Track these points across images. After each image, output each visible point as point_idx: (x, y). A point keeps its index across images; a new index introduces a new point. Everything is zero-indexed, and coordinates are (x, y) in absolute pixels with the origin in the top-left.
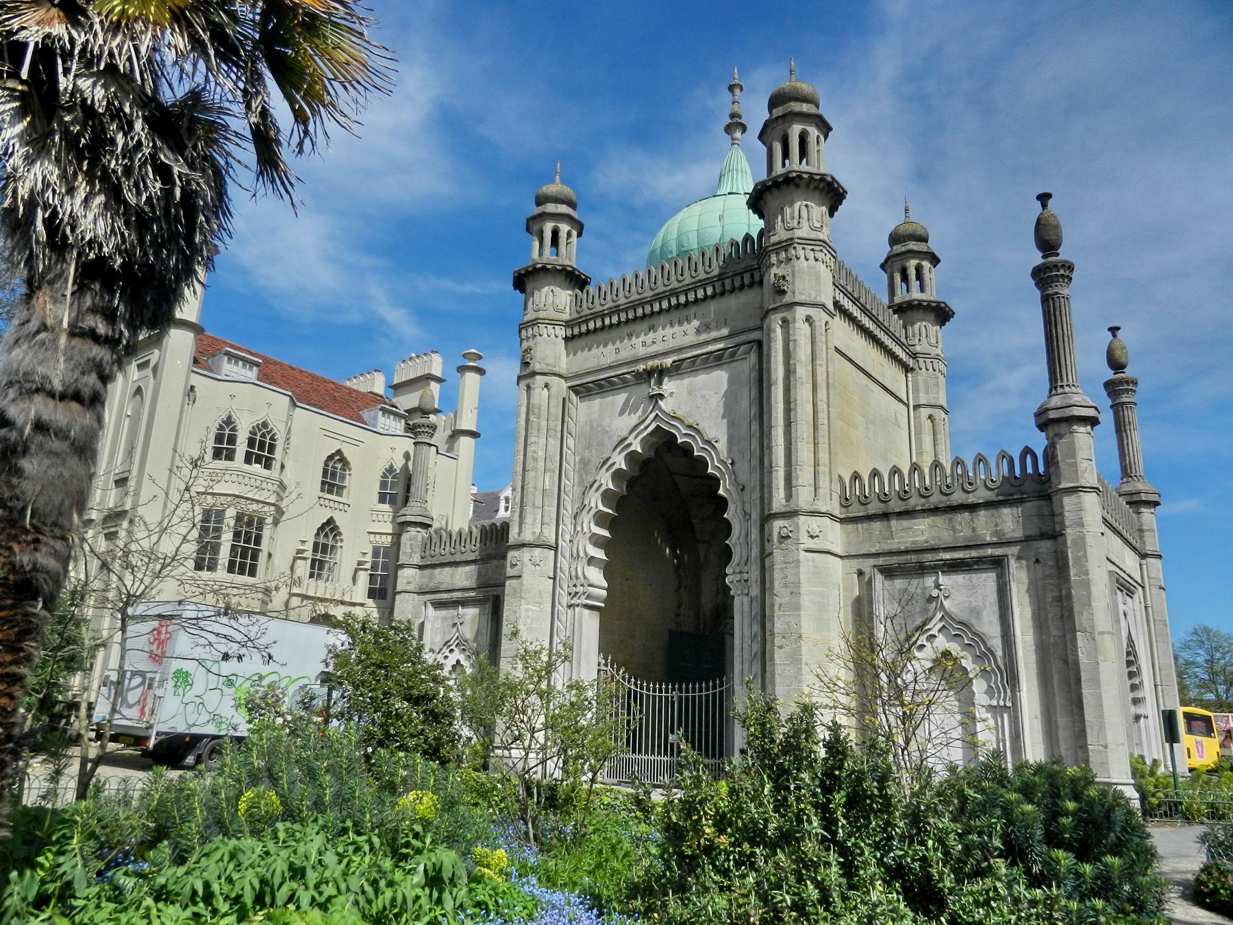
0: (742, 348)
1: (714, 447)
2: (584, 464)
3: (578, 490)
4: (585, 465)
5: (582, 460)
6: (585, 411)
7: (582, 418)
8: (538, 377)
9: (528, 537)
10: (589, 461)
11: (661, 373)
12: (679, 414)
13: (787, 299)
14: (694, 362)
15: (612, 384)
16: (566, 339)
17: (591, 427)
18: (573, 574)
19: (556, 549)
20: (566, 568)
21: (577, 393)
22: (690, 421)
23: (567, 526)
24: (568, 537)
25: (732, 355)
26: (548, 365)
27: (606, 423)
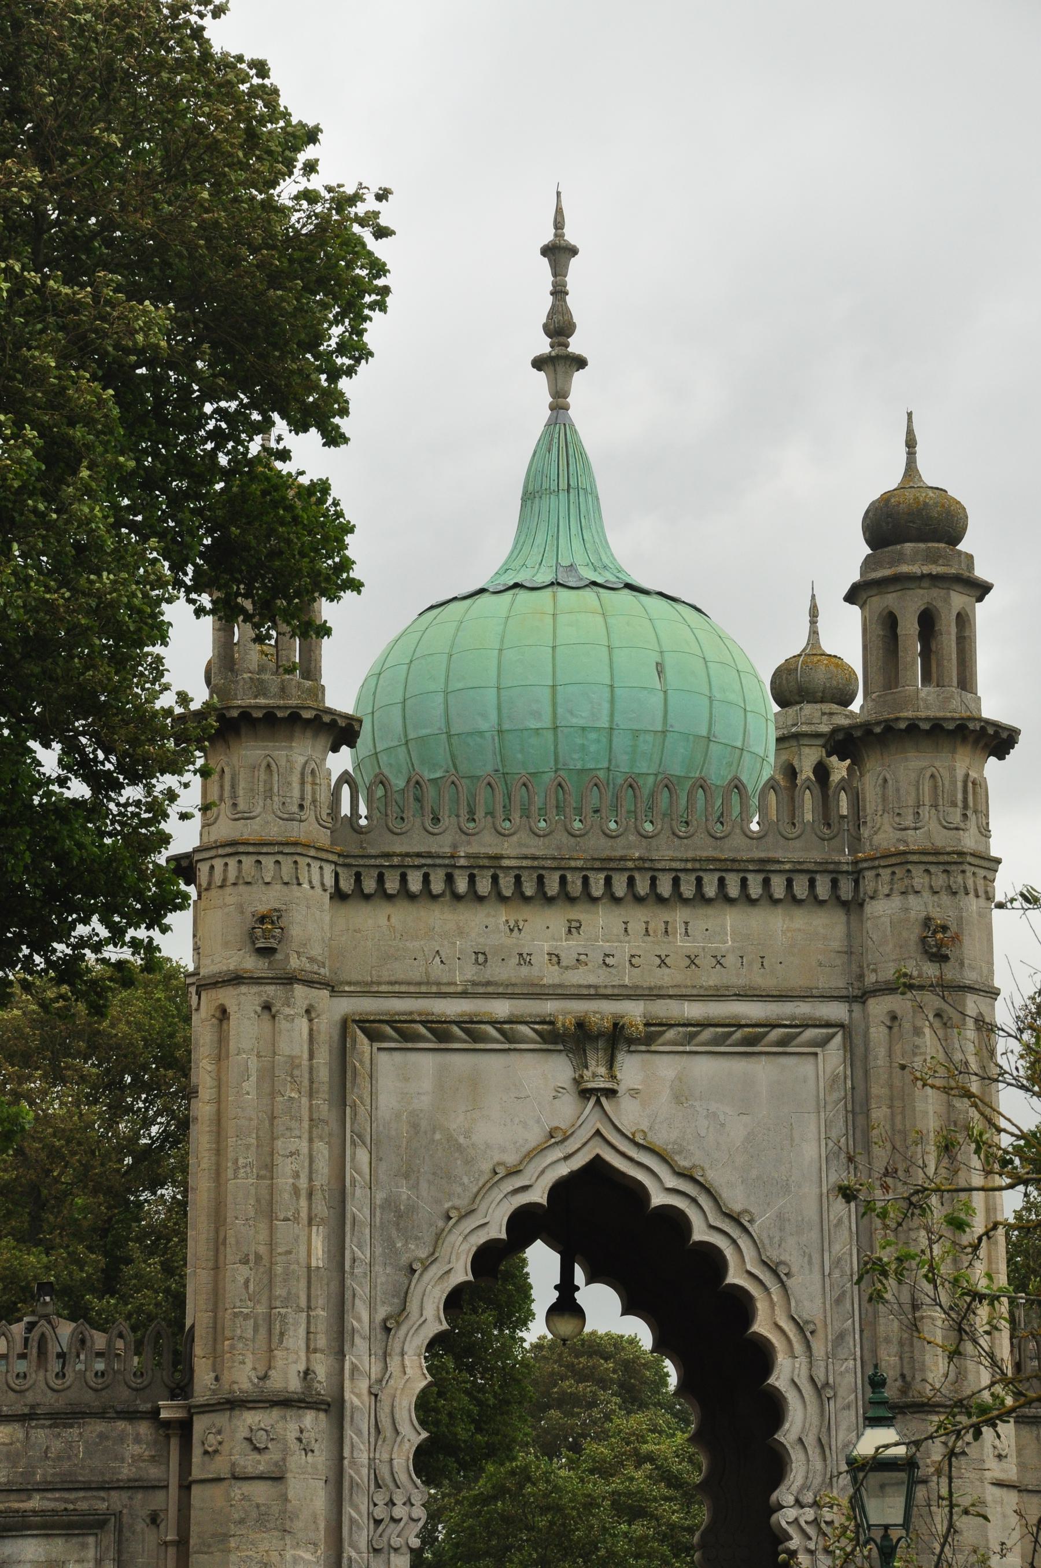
0: (810, 1033)
1: (745, 1230)
2: (398, 1216)
3: (385, 1276)
4: (400, 1216)
5: (390, 1204)
6: (402, 1083)
7: (388, 1101)
8: (299, 990)
9: (287, 1378)
10: (412, 1209)
11: (616, 1039)
12: (660, 1138)
13: (950, 973)
14: (692, 1036)
15: (475, 1037)
16: (339, 896)
17: (415, 1126)
18: (384, 1471)
19: (334, 1407)
20: (363, 1458)
21: (373, 1036)
22: (683, 1163)
23: (361, 1355)
24: (363, 1385)
25: (783, 1042)
26: (312, 960)
27: (456, 1122)
